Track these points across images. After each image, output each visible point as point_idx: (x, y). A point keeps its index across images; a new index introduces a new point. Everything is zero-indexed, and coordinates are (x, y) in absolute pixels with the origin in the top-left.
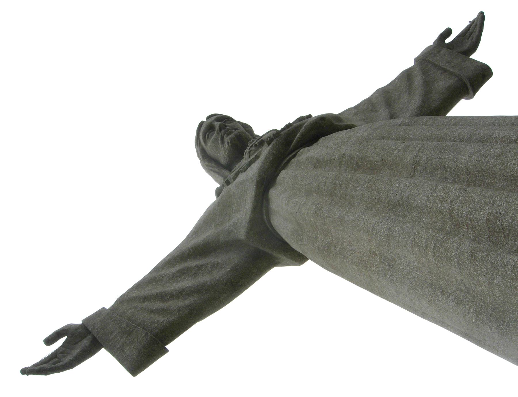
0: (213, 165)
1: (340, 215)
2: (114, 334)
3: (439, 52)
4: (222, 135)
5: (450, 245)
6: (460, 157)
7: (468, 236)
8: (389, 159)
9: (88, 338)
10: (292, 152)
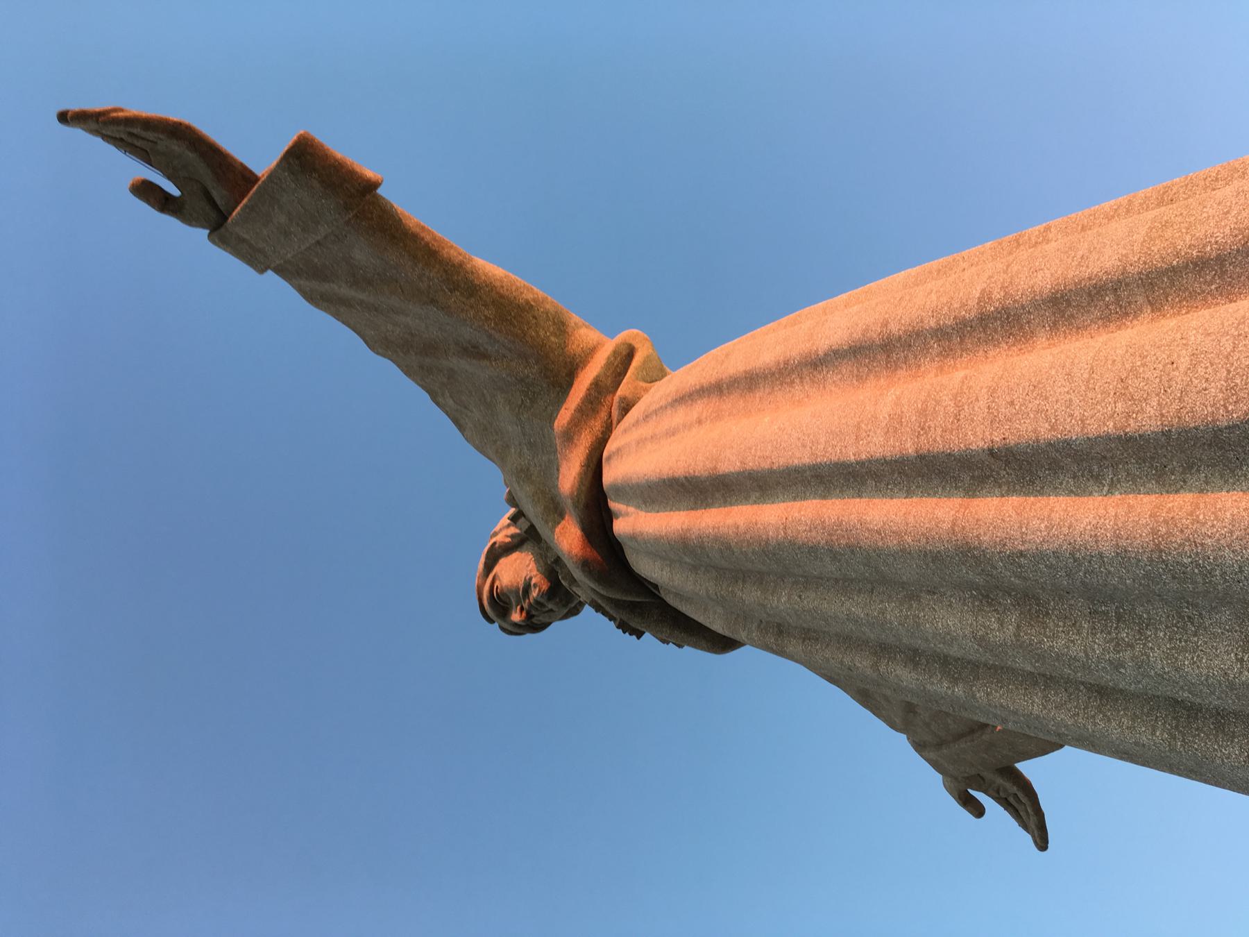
3: (244, 240)
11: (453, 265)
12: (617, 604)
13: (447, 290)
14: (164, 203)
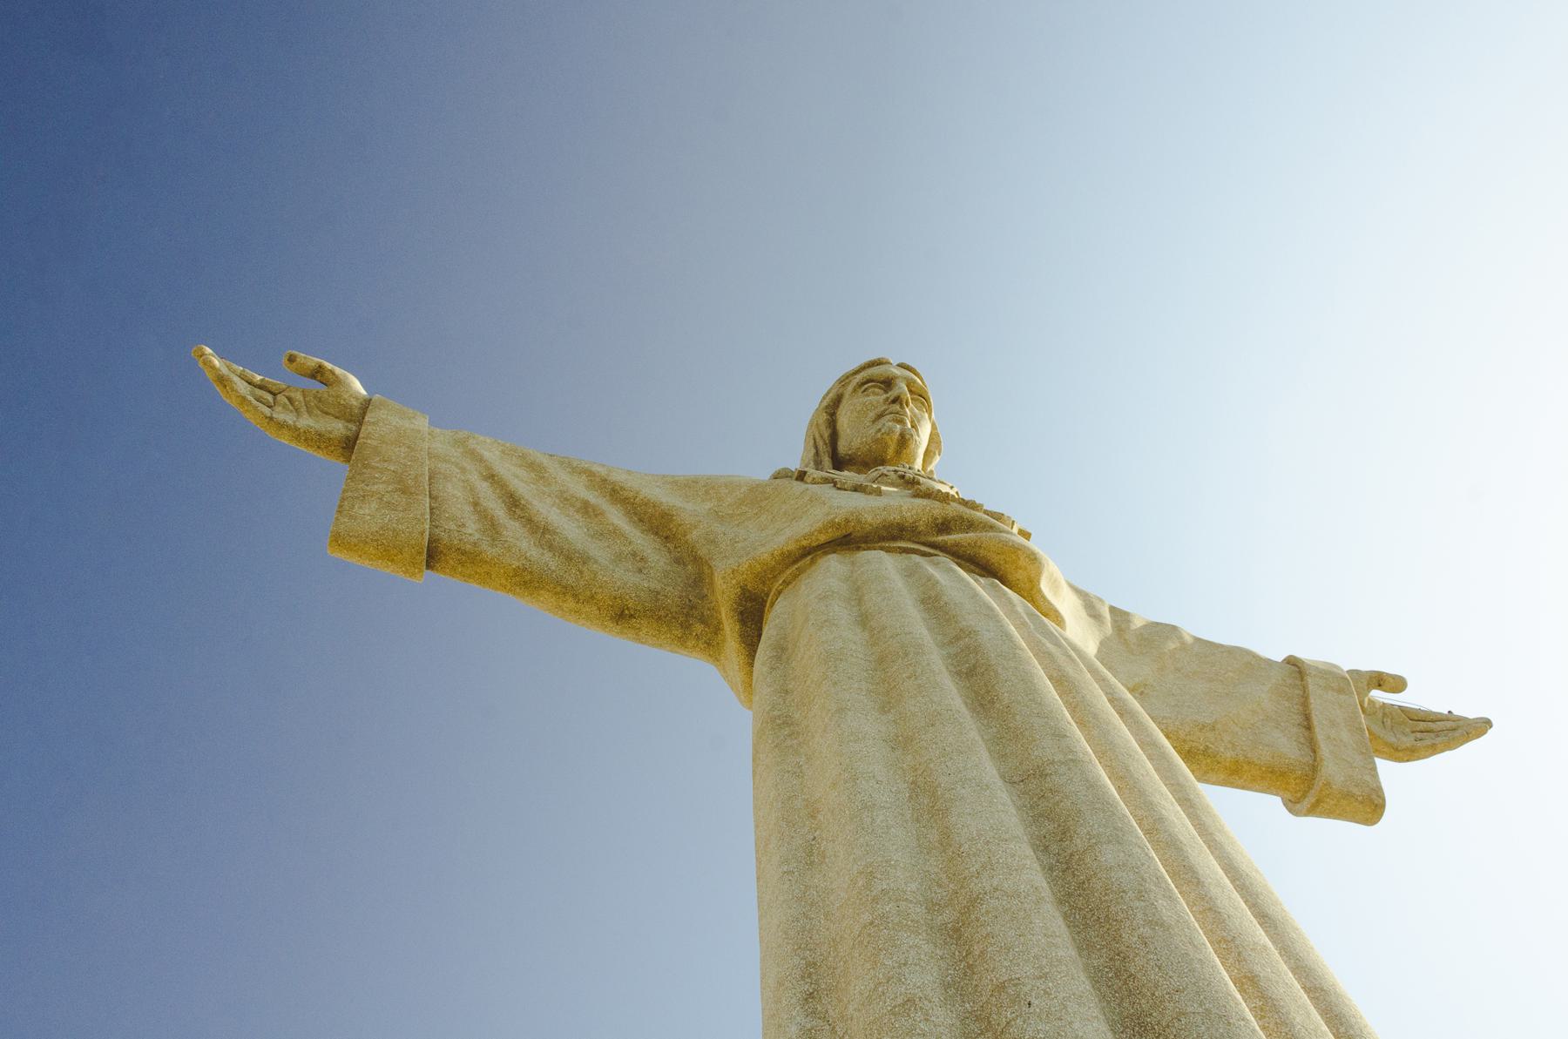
0: (826, 435)
1: (849, 700)
2: (386, 465)
4: (886, 410)
5: (904, 943)
6: (1104, 846)
7: (948, 969)
8: (1018, 717)
9: (350, 426)
10: (933, 546)
11: (1212, 770)
12: (970, 525)
13: (1210, 746)
14: (1380, 680)
